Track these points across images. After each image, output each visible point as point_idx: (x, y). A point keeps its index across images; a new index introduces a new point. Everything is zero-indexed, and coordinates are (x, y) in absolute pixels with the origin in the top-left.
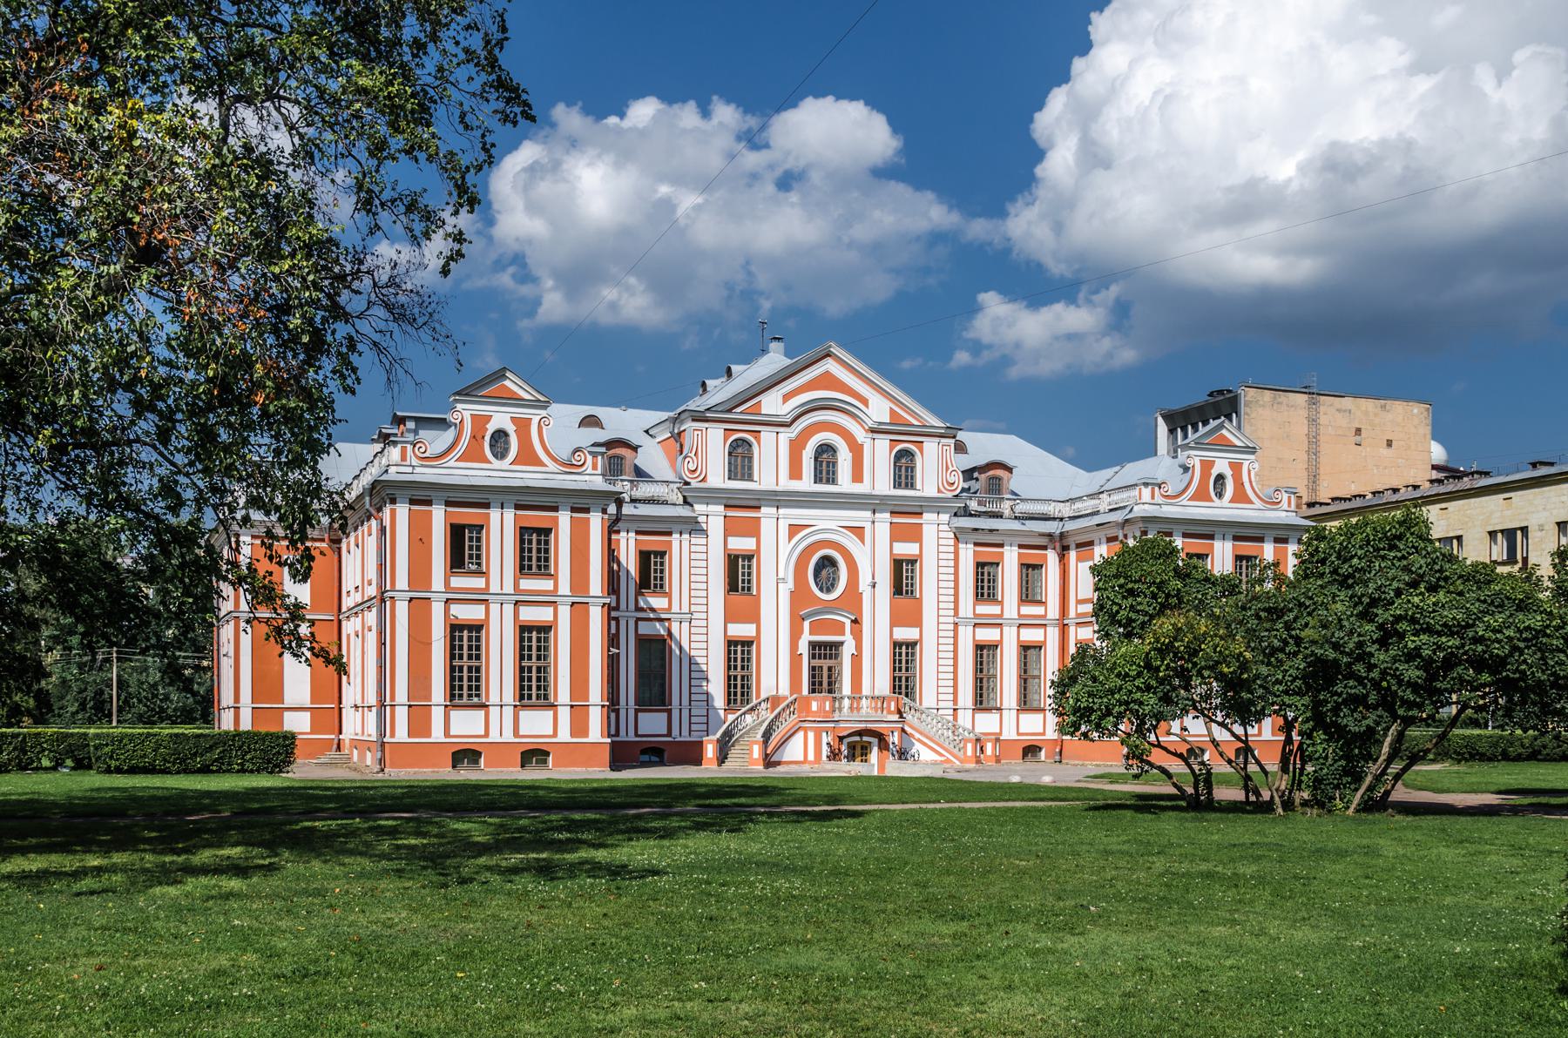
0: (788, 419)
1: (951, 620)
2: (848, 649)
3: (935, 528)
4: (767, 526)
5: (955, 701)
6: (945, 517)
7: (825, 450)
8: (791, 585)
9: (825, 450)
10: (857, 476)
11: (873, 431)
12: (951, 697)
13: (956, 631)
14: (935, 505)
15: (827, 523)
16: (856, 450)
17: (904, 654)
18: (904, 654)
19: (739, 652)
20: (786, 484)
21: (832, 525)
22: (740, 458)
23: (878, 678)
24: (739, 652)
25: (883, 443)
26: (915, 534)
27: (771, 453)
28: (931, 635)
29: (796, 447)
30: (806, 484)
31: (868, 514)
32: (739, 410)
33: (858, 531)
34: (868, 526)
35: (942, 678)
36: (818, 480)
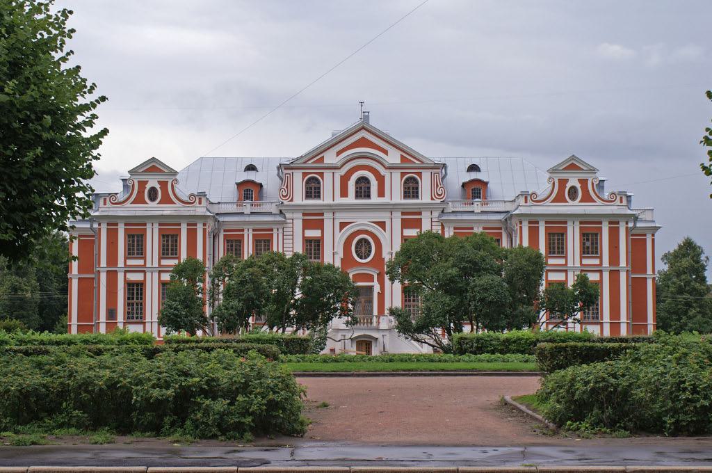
0: (339, 165)
2: (377, 289)
4: (328, 225)
7: (363, 181)
9: (363, 181)
10: (381, 193)
11: (390, 168)
14: (430, 208)
16: (381, 180)
20: (340, 200)
25: (397, 175)
27: (329, 184)
32: (310, 162)
33: (382, 225)
36: (358, 195)
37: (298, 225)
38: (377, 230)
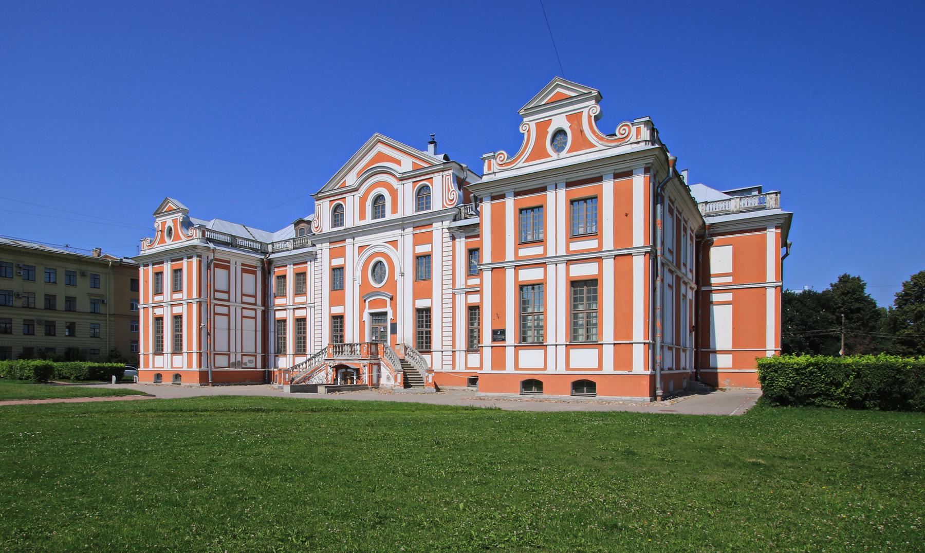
1: (451, 291)
2: (390, 316)
3: (439, 231)
5: (454, 345)
6: (447, 224)
7: (379, 198)
8: (359, 281)
9: (379, 198)
10: (394, 210)
11: (401, 179)
12: (451, 343)
13: (454, 298)
14: (439, 216)
15: (377, 241)
17: (423, 316)
18: (423, 316)
19: (338, 321)
21: (380, 242)
22: (338, 214)
23: (407, 332)
24: (338, 321)
26: (428, 239)
28: (437, 303)
29: (363, 200)
30: (369, 220)
31: (399, 231)
33: (394, 243)
34: (399, 238)
35: (447, 329)
36: (374, 217)
37: (326, 253)
38: (389, 250)
